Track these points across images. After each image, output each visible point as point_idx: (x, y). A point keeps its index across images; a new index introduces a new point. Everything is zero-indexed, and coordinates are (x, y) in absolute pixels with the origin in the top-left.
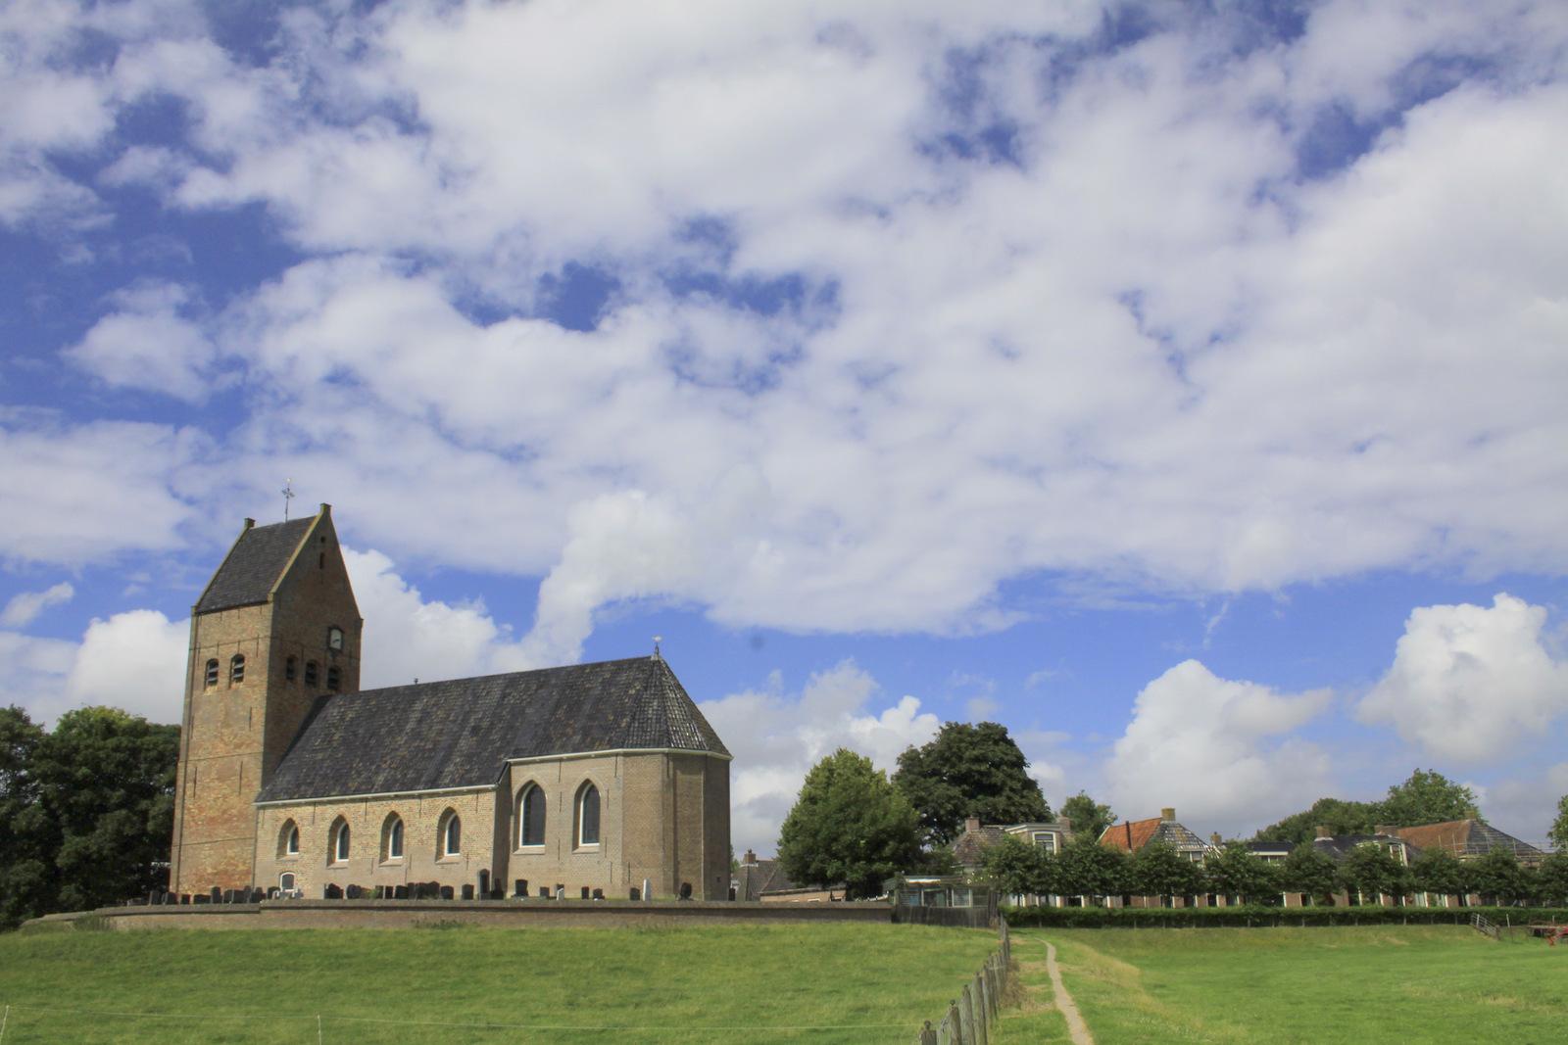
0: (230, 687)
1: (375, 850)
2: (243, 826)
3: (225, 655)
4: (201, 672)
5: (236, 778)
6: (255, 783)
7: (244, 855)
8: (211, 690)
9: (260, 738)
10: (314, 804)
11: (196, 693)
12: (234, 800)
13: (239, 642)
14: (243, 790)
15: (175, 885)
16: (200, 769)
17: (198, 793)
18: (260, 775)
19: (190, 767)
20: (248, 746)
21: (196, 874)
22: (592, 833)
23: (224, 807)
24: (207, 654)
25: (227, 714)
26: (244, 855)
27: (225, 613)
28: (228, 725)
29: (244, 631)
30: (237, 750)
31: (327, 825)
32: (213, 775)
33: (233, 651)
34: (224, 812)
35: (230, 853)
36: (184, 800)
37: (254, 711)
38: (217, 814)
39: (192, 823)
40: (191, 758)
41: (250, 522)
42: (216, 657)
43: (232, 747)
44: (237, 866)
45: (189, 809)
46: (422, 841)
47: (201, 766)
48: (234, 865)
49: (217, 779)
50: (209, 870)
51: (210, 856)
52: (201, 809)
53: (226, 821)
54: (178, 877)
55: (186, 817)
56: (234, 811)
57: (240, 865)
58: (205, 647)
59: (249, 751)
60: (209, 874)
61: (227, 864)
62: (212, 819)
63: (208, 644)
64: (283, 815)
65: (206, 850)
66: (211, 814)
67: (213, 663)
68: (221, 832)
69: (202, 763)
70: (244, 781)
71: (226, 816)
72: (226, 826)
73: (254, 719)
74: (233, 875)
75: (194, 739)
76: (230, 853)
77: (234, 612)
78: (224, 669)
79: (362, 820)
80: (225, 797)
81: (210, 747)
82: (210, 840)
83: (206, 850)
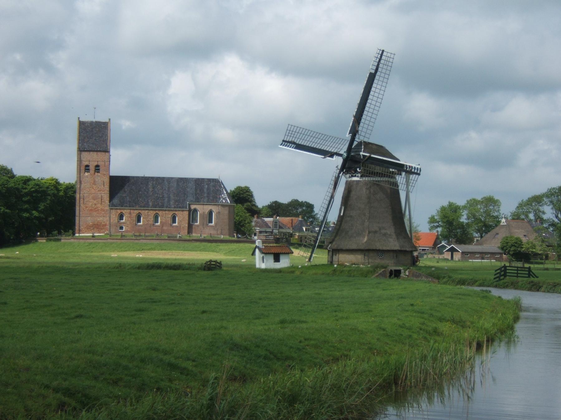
0: (95, 174)
4: (83, 168)
5: (100, 200)
7: (104, 220)
8: (86, 174)
9: (108, 189)
10: (130, 209)
11: (82, 174)
12: (99, 205)
13: (98, 161)
16: (85, 196)
17: (85, 202)
18: (108, 199)
19: (81, 195)
20: (103, 191)
22: (210, 221)
23: (95, 207)
24: (87, 163)
28: (95, 185)
32: (90, 197)
33: (96, 164)
34: (95, 208)
36: (80, 204)
37: (105, 182)
39: (83, 211)
40: (81, 192)
41: (79, 118)
44: (101, 223)
47: (85, 195)
50: (91, 224)
53: (96, 211)
54: (79, 225)
55: (81, 209)
58: (84, 161)
59: (103, 192)
63: (85, 160)
64: (119, 211)
67: (87, 166)
68: (95, 214)
69: (86, 194)
70: (103, 200)
72: (96, 212)
73: (105, 184)
78: (92, 168)
80: (95, 204)
81: (89, 190)
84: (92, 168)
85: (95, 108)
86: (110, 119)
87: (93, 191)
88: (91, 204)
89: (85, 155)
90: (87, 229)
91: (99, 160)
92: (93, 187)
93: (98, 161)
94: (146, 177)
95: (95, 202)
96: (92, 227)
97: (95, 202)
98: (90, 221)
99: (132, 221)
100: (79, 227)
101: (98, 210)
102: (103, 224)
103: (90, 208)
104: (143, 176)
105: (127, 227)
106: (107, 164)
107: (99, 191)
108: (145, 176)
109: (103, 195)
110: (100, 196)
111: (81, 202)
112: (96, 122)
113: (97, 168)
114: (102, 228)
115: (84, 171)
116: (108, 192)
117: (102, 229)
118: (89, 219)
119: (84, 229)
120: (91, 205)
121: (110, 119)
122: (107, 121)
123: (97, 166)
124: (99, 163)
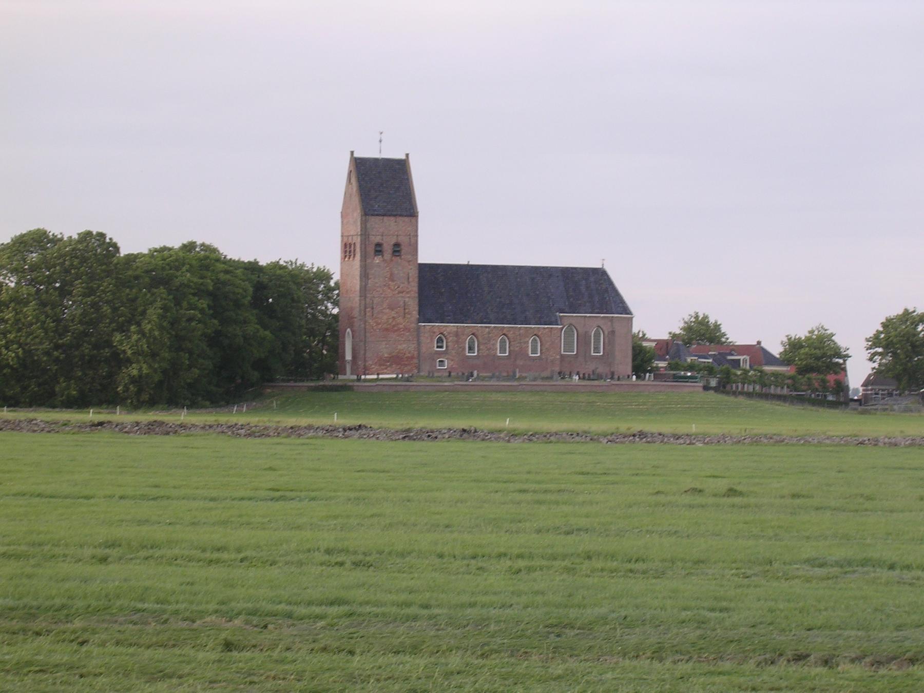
4: (371, 249)
8: (377, 260)
9: (416, 289)
11: (369, 261)
12: (400, 320)
16: (375, 302)
17: (375, 315)
18: (417, 309)
20: (408, 293)
24: (378, 239)
27: (385, 218)
28: (393, 281)
32: (385, 306)
34: (394, 326)
37: (410, 275)
40: (368, 295)
41: (352, 153)
42: (381, 241)
50: (386, 355)
53: (396, 331)
56: (401, 326)
62: (387, 330)
63: (374, 233)
67: (379, 245)
71: (396, 328)
72: (396, 333)
73: (411, 280)
75: (369, 285)
76: (399, 347)
77: (392, 218)
78: (388, 249)
80: (393, 318)
84: (388, 249)
85: (381, 133)
86: (407, 155)
88: (385, 317)
89: (374, 221)
91: (400, 232)
92: (389, 285)
93: (397, 236)
94: (472, 266)
95: (393, 314)
97: (393, 314)
98: (384, 350)
99: (460, 349)
101: (399, 329)
103: (385, 326)
104: (247, 258)
105: (452, 360)
106: (413, 241)
107: (399, 293)
108: (470, 263)
109: (407, 300)
110: (401, 303)
111: (368, 314)
112: (382, 159)
113: (397, 249)
115: (372, 253)
116: (417, 295)
117: (406, 365)
121: (407, 155)
122: (404, 157)
123: (397, 245)
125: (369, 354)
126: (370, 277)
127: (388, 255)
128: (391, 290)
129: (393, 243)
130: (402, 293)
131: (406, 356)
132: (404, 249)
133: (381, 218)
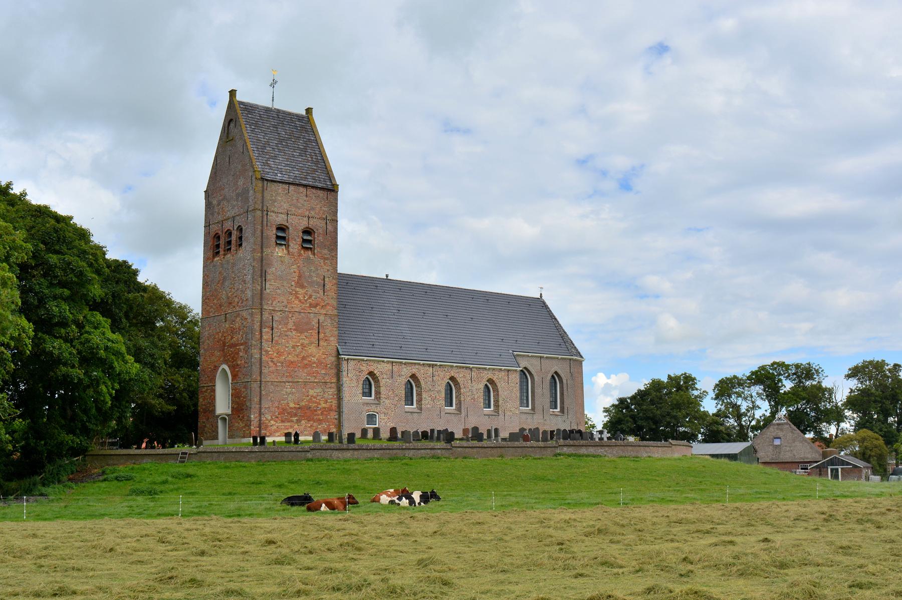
1: (441, 402)
2: (323, 372)
3: (297, 224)
4: (272, 233)
6: (332, 339)
7: (326, 396)
8: (280, 252)
11: (267, 251)
12: (313, 349)
14: (321, 343)
15: (257, 415)
16: (276, 318)
17: (275, 339)
19: (266, 315)
21: (278, 408)
23: (303, 354)
24: (280, 219)
25: (300, 277)
26: (326, 396)
28: (302, 287)
29: (313, 209)
30: (313, 309)
31: (403, 380)
32: (291, 326)
33: (304, 224)
34: (304, 358)
35: (311, 392)
37: (327, 279)
38: (296, 359)
39: (271, 364)
40: (265, 307)
43: (308, 305)
45: (267, 351)
46: (474, 399)
48: (316, 402)
49: (294, 330)
50: (292, 405)
51: (292, 393)
52: (280, 354)
53: (306, 366)
54: (260, 408)
56: (314, 359)
57: (322, 402)
60: (291, 408)
61: (310, 401)
63: (276, 210)
65: (288, 388)
66: (290, 358)
67: (281, 228)
68: (302, 375)
69: (279, 313)
70: (322, 335)
71: (306, 362)
73: (327, 287)
74: (316, 411)
75: (268, 291)
76: (311, 392)
79: (431, 379)
82: (290, 380)
83: (288, 388)
87: (296, 305)
88: (291, 343)
90: (283, 421)
91: (313, 213)
92: (297, 293)
93: (309, 217)
96: (296, 415)
100: (260, 414)
101: (310, 365)
102: (324, 405)
106: (330, 227)
107: (311, 306)
109: (322, 318)
110: (314, 323)
111: (265, 337)
114: (321, 418)
118: (289, 390)
119: (272, 422)
120: (293, 347)
123: (307, 231)
124: (313, 223)
125: (265, 404)
126: (268, 277)
127: (295, 246)
128: (300, 301)
129: (302, 228)
130: (315, 307)
131: (320, 407)
132: (319, 239)
133: (286, 186)
